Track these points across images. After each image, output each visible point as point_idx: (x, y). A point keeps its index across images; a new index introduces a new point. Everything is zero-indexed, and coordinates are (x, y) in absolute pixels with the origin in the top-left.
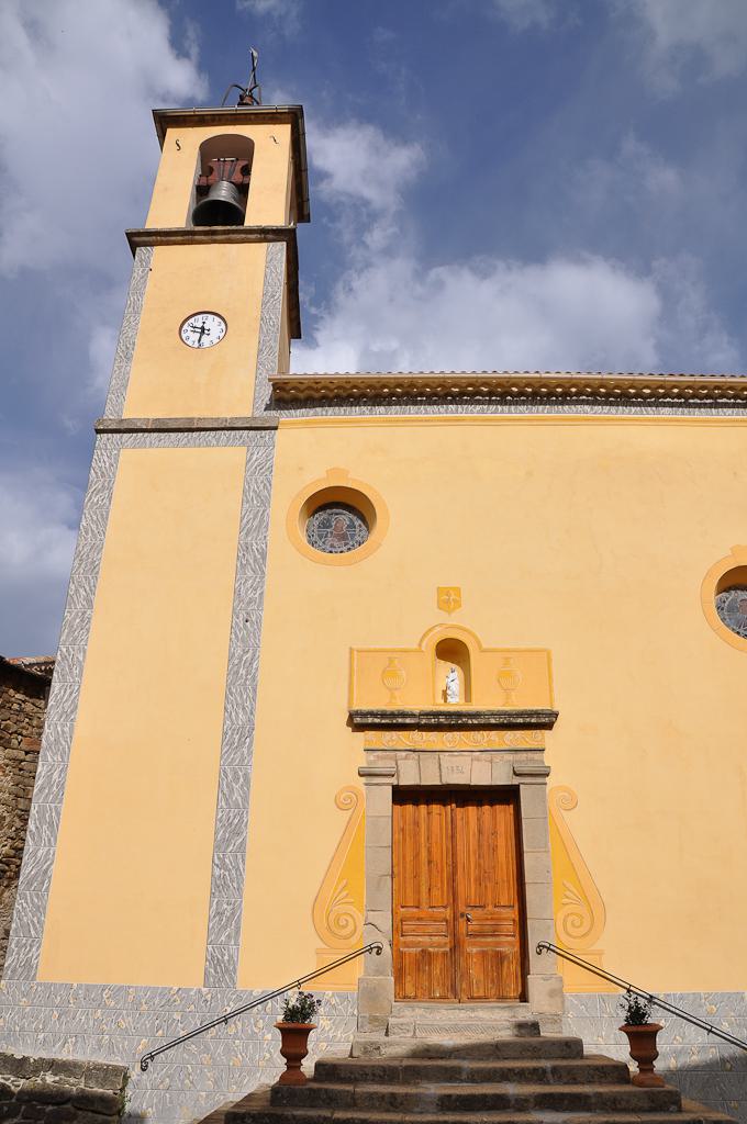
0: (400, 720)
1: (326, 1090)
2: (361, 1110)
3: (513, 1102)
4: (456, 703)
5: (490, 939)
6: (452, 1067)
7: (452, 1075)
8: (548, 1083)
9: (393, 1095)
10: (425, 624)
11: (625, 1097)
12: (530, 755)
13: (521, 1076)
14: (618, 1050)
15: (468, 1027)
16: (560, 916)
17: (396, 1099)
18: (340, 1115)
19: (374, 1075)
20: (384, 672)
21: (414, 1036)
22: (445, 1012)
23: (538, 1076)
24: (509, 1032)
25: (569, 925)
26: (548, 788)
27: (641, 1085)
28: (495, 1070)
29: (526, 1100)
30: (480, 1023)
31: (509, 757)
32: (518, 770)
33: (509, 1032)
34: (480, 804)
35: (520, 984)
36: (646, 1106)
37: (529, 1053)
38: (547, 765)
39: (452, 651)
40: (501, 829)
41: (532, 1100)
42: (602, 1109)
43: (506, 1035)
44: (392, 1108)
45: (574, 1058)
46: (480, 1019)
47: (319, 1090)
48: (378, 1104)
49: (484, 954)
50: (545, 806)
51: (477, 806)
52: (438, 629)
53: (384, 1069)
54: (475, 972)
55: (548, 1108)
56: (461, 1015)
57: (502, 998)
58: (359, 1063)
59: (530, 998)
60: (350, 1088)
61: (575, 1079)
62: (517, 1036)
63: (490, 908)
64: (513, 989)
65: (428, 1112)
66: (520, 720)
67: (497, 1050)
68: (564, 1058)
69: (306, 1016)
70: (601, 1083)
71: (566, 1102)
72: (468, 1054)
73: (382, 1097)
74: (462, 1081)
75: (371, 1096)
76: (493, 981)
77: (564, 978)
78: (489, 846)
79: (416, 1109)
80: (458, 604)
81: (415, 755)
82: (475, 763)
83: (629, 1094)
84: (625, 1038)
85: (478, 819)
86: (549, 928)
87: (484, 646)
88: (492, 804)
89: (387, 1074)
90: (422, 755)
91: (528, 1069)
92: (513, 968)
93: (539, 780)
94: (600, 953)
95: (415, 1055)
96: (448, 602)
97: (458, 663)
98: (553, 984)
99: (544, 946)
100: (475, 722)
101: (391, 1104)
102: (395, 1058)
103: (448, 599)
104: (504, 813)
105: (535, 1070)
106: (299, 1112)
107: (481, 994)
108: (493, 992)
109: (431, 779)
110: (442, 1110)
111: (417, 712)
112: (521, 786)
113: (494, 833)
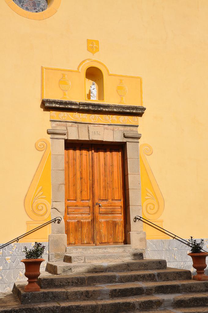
0: (69, 106)
1: (52, 293)
2: (71, 301)
3: (145, 291)
4: (94, 100)
5: (110, 215)
6: (111, 276)
7: (111, 280)
8: (156, 281)
9: (87, 292)
10: (79, 59)
11: (195, 286)
12: (132, 128)
13: (144, 278)
14: (188, 265)
15: (110, 257)
16: (144, 205)
17: (88, 293)
18: (64, 304)
19: (72, 282)
20: (59, 81)
21: (85, 262)
22: (92, 250)
23: (151, 278)
24: (130, 258)
25: (148, 209)
26: (140, 144)
27: (199, 280)
28: (132, 276)
29: (151, 290)
30: (116, 254)
31: (122, 128)
32: (126, 135)
33: (130, 258)
34: (105, 151)
35: (124, 236)
36: (204, 289)
37: (143, 267)
38: (139, 133)
39: (94, 74)
40: (115, 163)
41: (154, 289)
42: (185, 292)
43: (128, 259)
44: (86, 298)
45: (163, 269)
46: (109, 253)
47: (49, 292)
48: (79, 297)
49: (107, 222)
50: (138, 153)
51: (104, 152)
52: (88, 61)
53: (78, 279)
54: (104, 231)
55: (161, 293)
56: (100, 251)
57: (116, 243)
58: (60, 277)
59: (131, 242)
60: (63, 290)
61: (168, 278)
62: (133, 260)
63: (110, 200)
64: (121, 238)
65: (105, 299)
66: (128, 111)
67: (127, 267)
68: (158, 269)
69: (38, 256)
70: (179, 280)
71: (169, 290)
72: (114, 269)
73: (82, 293)
74: (116, 282)
75: (76, 293)
76: (111, 235)
77: (146, 233)
78: (110, 171)
79: (99, 298)
80: (97, 49)
81: (76, 125)
82: (106, 130)
83: (197, 284)
84: (190, 258)
85: (104, 158)
86: (139, 209)
87: (110, 73)
88: (111, 151)
89: (79, 281)
90: (89, 125)
91: (147, 275)
92: (120, 229)
93: (136, 140)
94: (162, 221)
95: (89, 271)
96: (92, 47)
97: (95, 81)
98: (141, 235)
99: (138, 218)
100: (107, 110)
101: (86, 296)
102: (79, 273)
103: (93, 46)
104: (116, 156)
105: (150, 275)
106: (42, 306)
107: (106, 241)
108: (111, 240)
109: (84, 137)
110: (112, 297)
111: (78, 103)
112: (127, 143)
113: (112, 165)
